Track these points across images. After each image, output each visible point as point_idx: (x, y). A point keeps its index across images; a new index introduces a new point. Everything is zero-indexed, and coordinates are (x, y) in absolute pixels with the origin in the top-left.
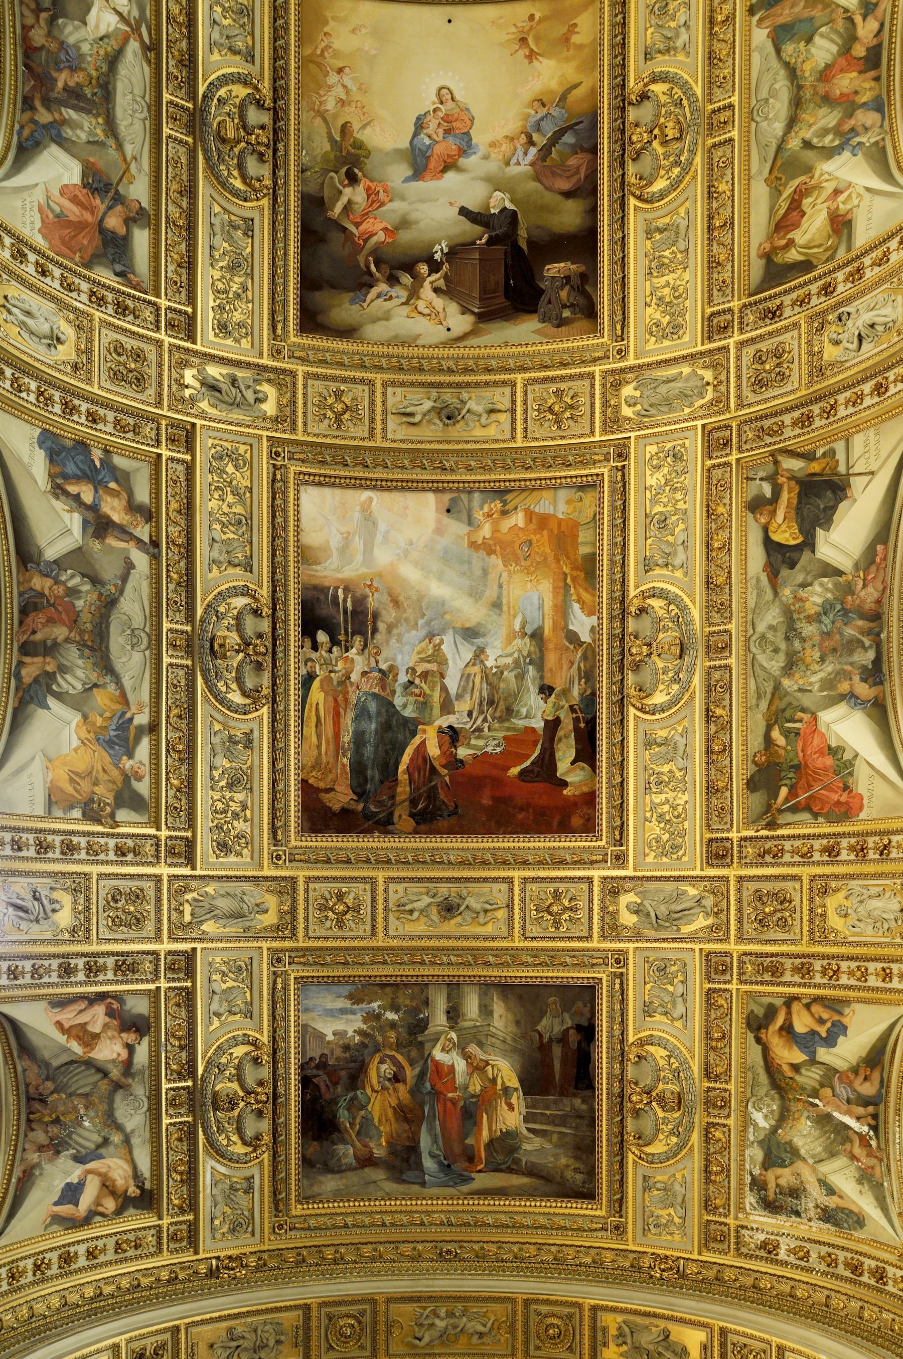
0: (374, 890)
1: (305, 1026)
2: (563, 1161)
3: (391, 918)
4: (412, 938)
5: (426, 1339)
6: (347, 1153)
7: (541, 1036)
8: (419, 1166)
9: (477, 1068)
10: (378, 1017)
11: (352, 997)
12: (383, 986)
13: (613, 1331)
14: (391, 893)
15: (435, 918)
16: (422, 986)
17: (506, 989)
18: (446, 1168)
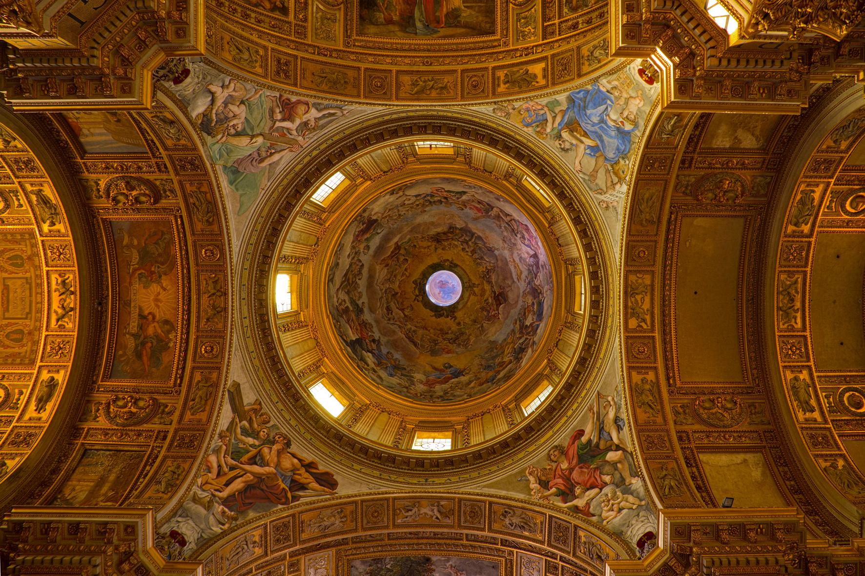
13: (502, 78)
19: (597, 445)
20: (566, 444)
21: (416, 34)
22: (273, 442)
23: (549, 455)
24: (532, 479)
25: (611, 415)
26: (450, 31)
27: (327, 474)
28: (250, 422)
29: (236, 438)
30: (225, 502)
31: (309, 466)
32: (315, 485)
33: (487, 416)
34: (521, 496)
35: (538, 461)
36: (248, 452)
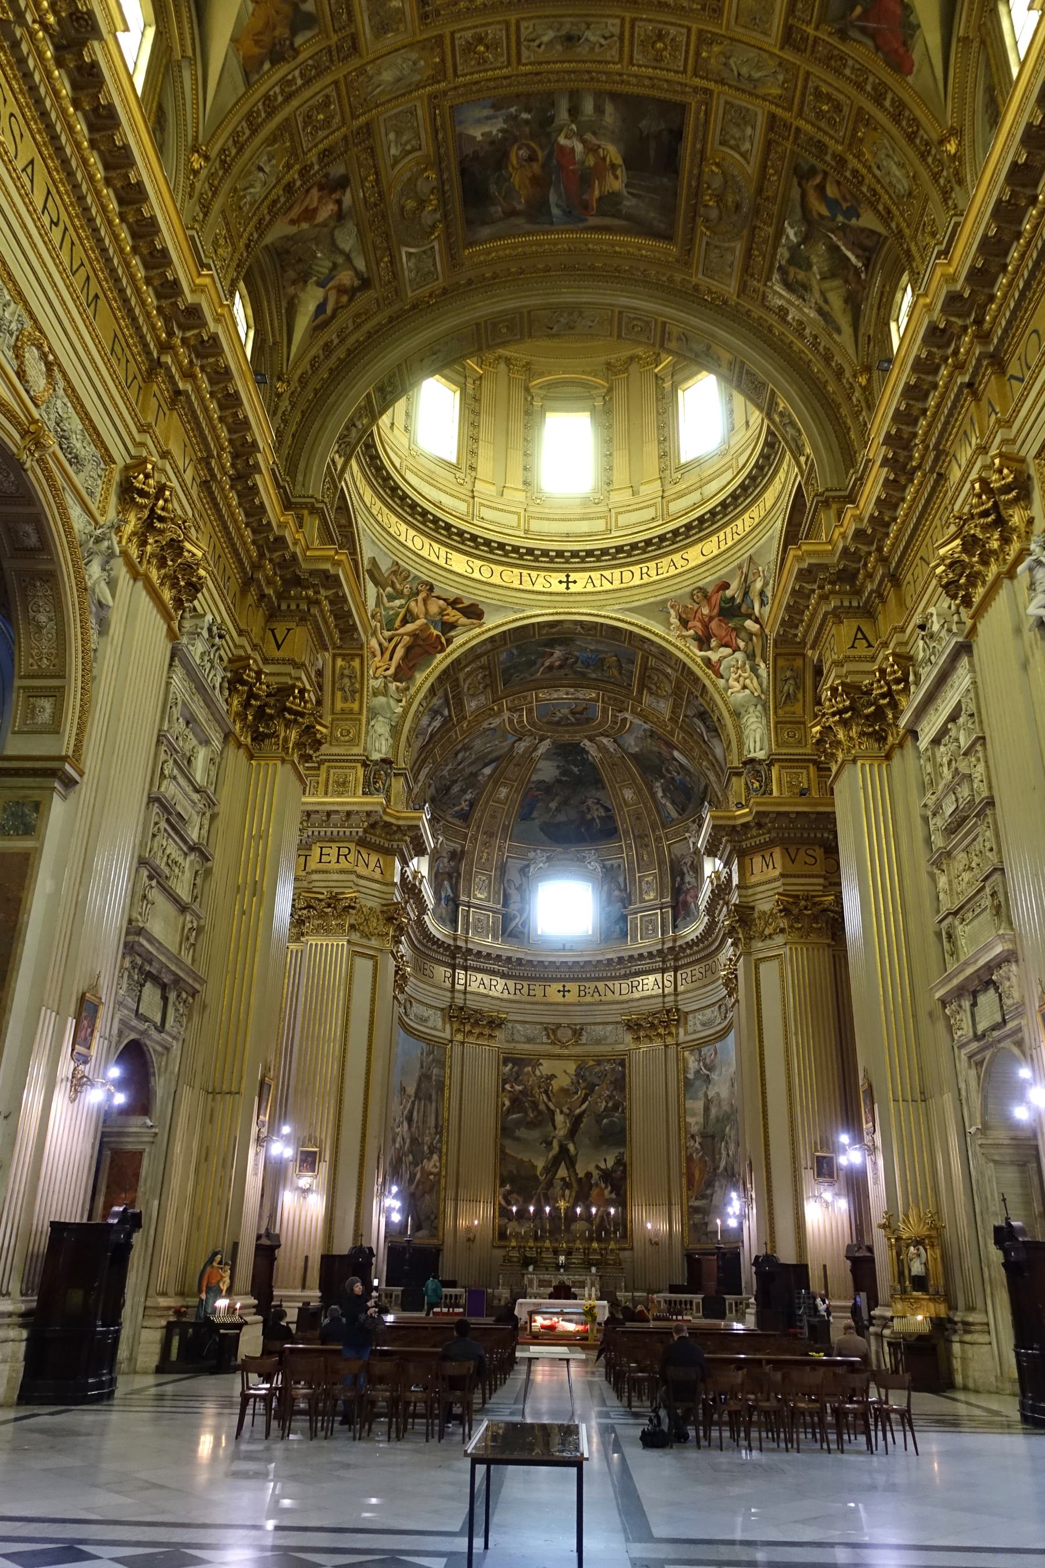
0: (508, 30)
1: (460, 135)
2: (652, 215)
3: (523, 48)
4: (540, 63)
5: (556, 328)
6: (497, 210)
7: (641, 132)
8: (549, 213)
9: (591, 149)
10: (514, 118)
11: (496, 106)
12: (518, 96)
14: (522, 29)
15: (559, 47)
16: (550, 94)
17: (614, 96)
18: (568, 213)
19: (740, 606)
20: (710, 590)
21: (552, 223)
22: (418, 594)
23: (692, 595)
24: (673, 613)
25: (759, 584)
26: (607, 221)
27: (472, 605)
28: (393, 585)
29: (386, 609)
30: (396, 677)
31: (454, 603)
32: (463, 620)
33: (634, 368)
34: (659, 629)
35: (681, 596)
36: (398, 614)
